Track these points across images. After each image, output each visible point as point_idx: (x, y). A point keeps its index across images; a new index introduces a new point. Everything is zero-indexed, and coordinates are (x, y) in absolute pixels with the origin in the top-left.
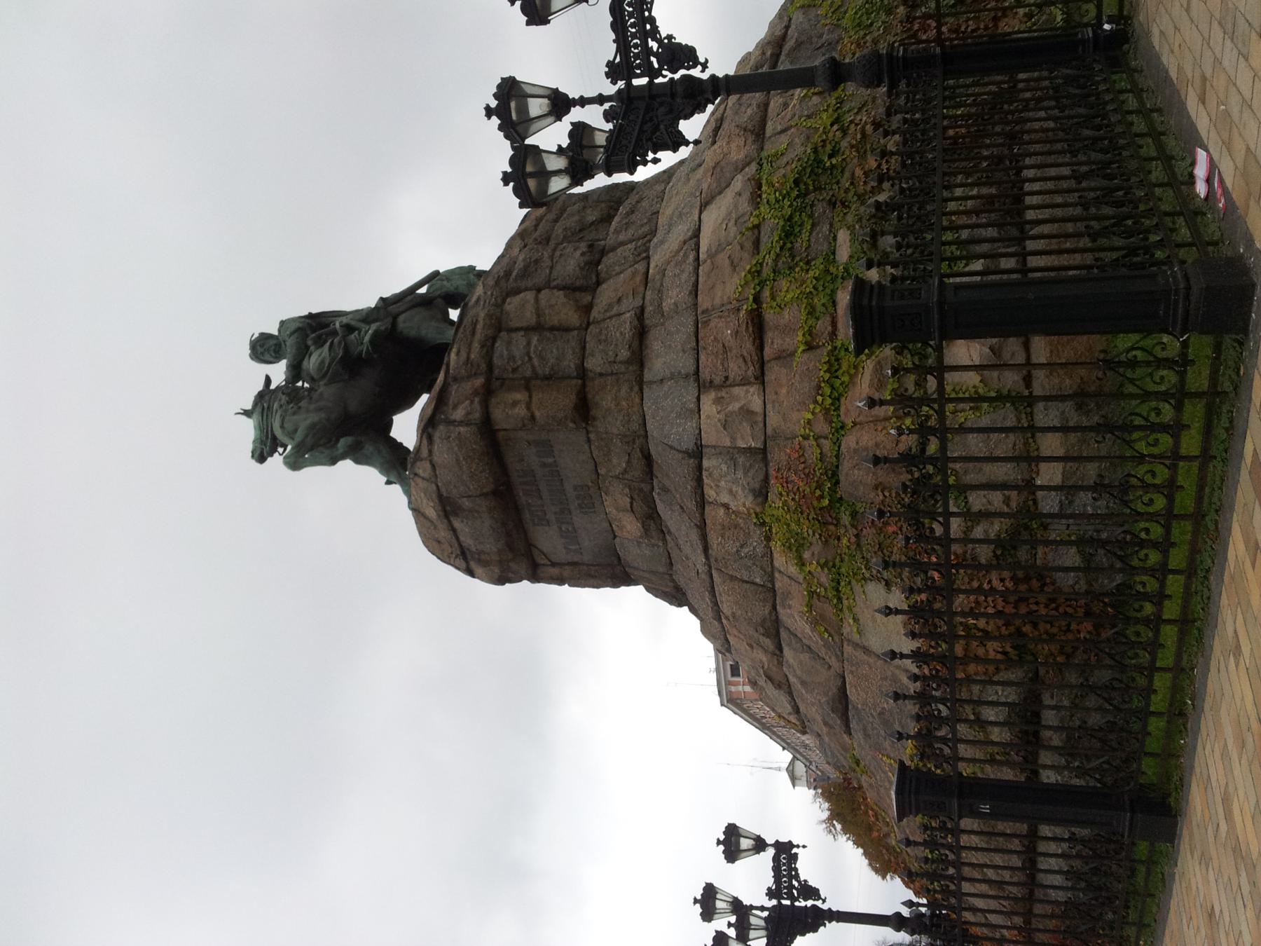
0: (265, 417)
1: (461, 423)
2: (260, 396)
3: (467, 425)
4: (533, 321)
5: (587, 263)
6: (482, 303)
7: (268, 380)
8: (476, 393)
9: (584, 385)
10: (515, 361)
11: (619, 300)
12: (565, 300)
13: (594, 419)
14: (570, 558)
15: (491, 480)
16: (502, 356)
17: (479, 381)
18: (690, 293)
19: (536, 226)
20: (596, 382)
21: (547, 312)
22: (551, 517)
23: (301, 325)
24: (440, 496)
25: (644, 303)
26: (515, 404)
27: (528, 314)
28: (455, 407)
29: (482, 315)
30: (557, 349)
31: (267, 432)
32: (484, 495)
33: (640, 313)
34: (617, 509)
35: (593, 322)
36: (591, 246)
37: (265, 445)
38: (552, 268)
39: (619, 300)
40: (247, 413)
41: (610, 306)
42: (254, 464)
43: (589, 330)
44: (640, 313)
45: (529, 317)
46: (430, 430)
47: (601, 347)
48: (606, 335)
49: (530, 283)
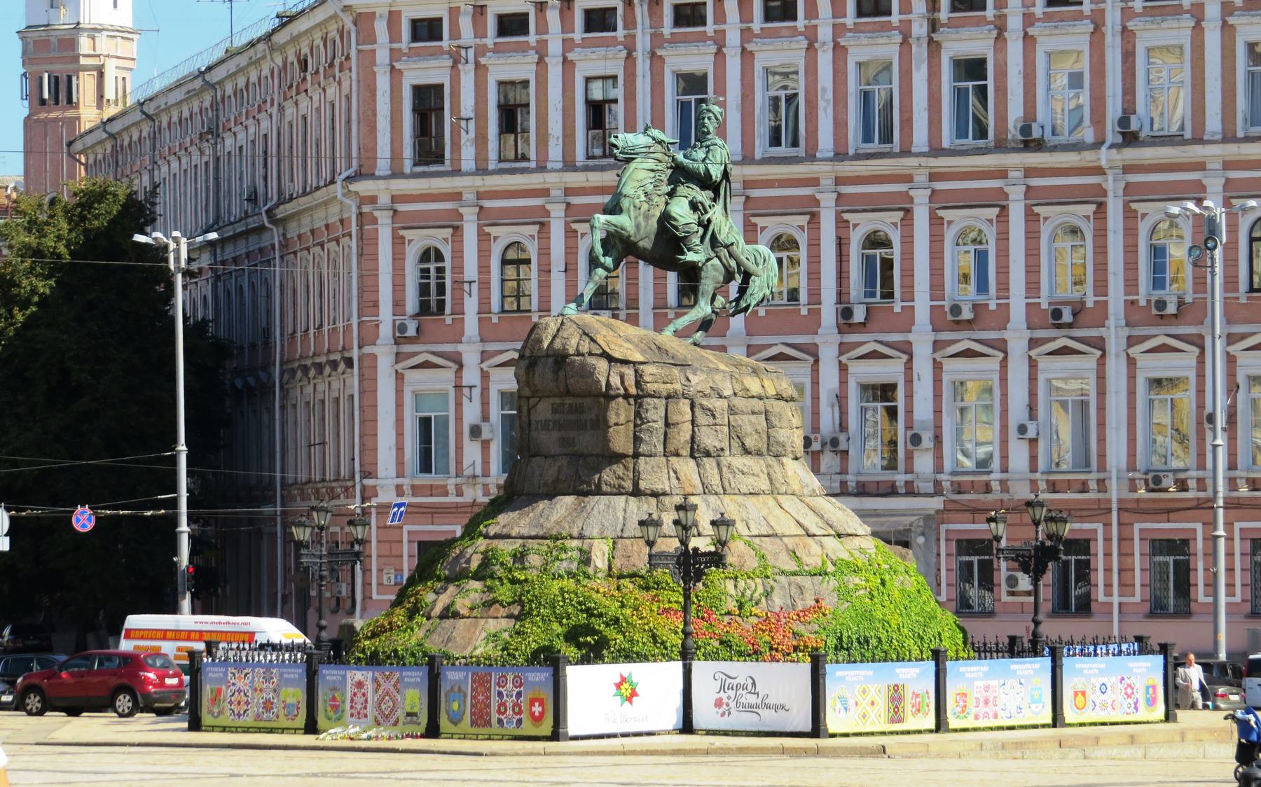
0: (644, 150)
1: (608, 381)
4: (670, 421)
8: (625, 389)
9: (628, 456)
11: (678, 478)
14: (533, 422)
17: (633, 391)
19: (753, 397)
22: (557, 417)
23: (714, 177)
29: (678, 386)
33: (664, 494)
34: (560, 467)
35: (668, 460)
36: (722, 450)
39: (678, 478)
41: (675, 472)
44: (664, 494)
45: (674, 418)
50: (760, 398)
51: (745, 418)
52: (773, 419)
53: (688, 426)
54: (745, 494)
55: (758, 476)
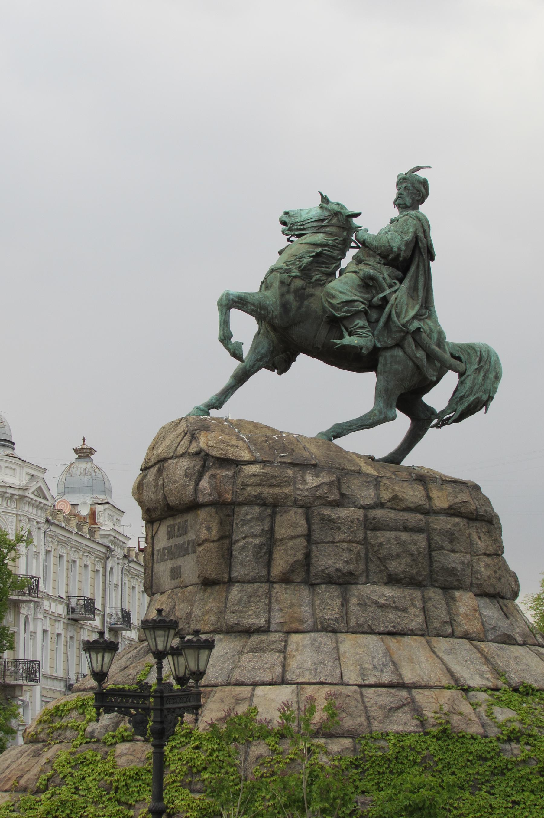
0: (316, 224)
2: (337, 214)
3: (196, 490)
4: (278, 536)
5: (328, 575)
6: (300, 487)
7: (357, 215)
8: (220, 495)
9: (224, 583)
10: (243, 525)
12: (290, 563)
13: (205, 591)
15: (173, 504)
16: (247, 514)
17: (228, 497)
18: (237, 680)
20: (224, 594)
21: (283, 548)
22: (172, 542)
23: (395, 249)
24: (165, 460)
25: (272, 632)
26: (209, 529)
27: (283, 531)
28: (214, 476)
29: (288, 490)
30: (249, 561)
31: (300, 230)
32: (165, 498)
33: (261, 631)
37: (288, 230)
38: (333, 542)
40: (325, 199)
42: (281, 214)
43: (266, 586)
45: (281, 532)
46: (203, 454)
47: (245, 598)
48: (253, 602)
49: (315, 527)
50: (418, 509)
51: (393, 534)
52: (437, 538)
53: (302, 541)
54: (379, 633)
55: (404, 610)
